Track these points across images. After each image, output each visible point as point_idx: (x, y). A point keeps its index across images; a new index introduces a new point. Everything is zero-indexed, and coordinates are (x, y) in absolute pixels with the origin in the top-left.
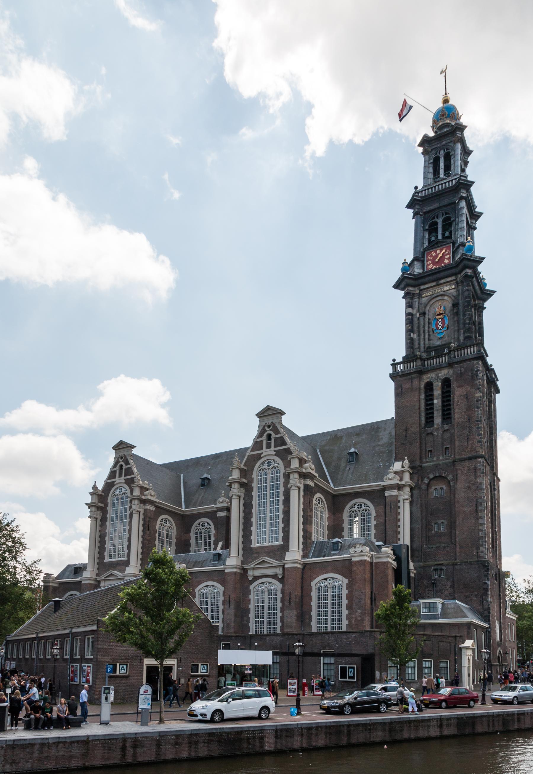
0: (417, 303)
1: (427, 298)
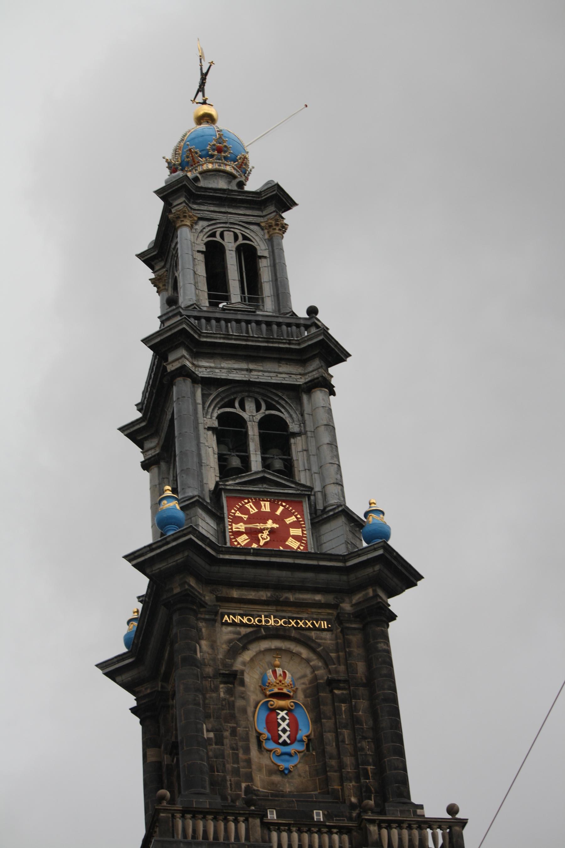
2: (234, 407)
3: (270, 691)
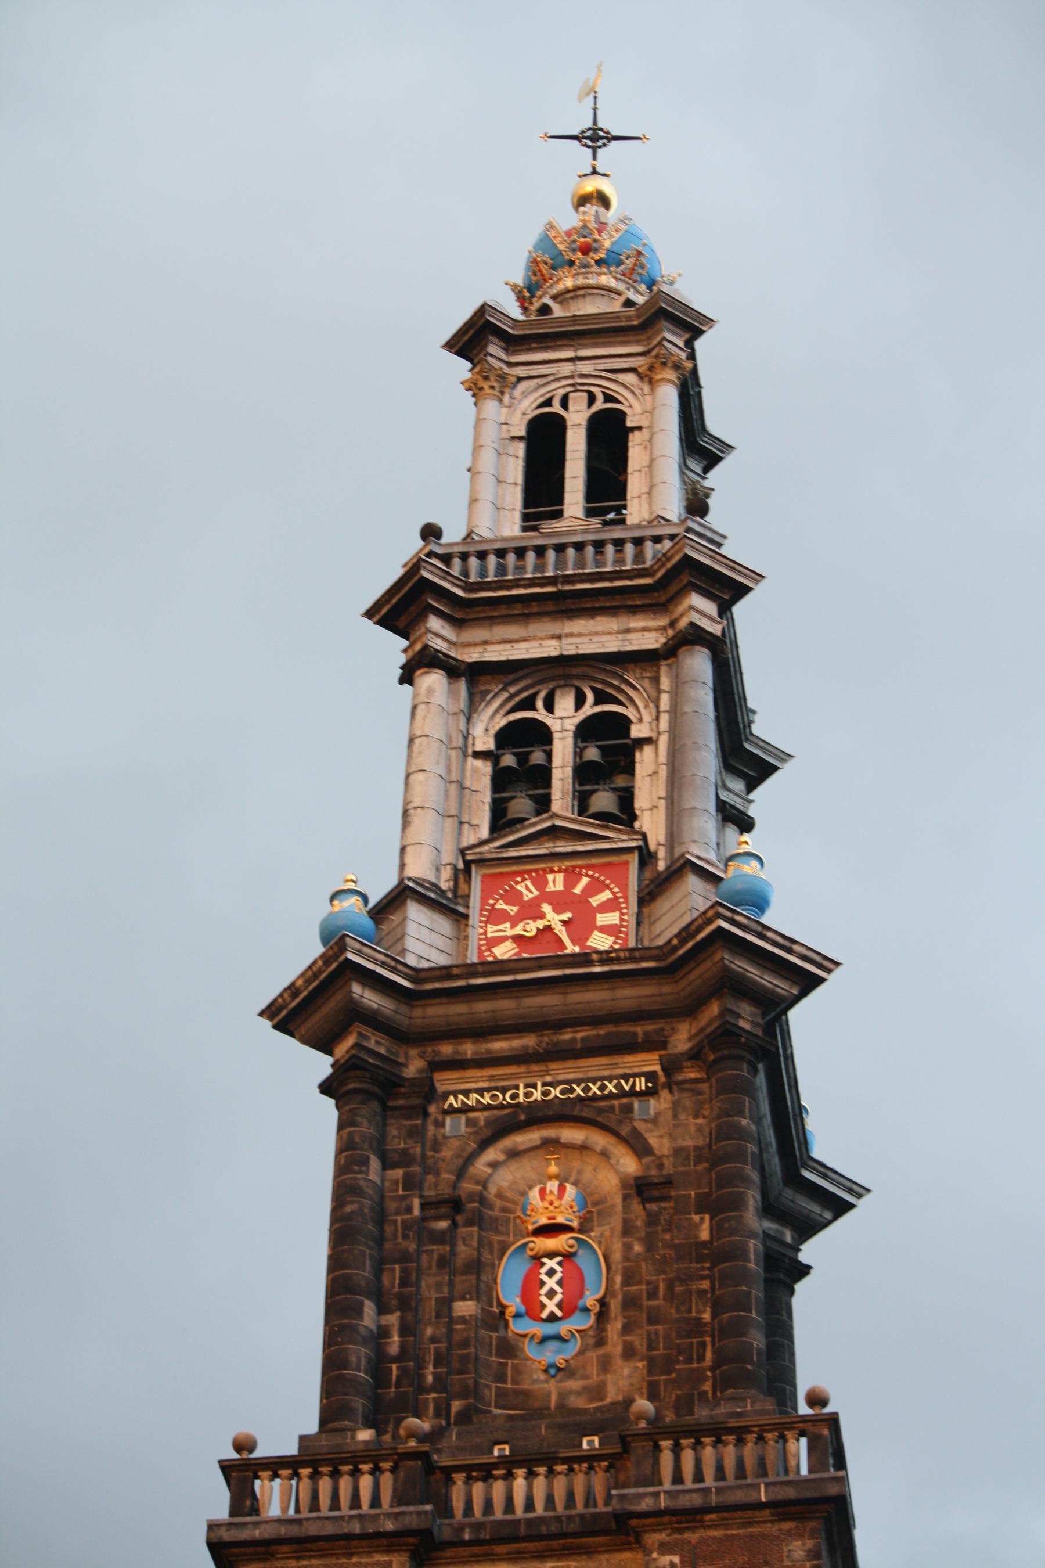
2: (534, 709)
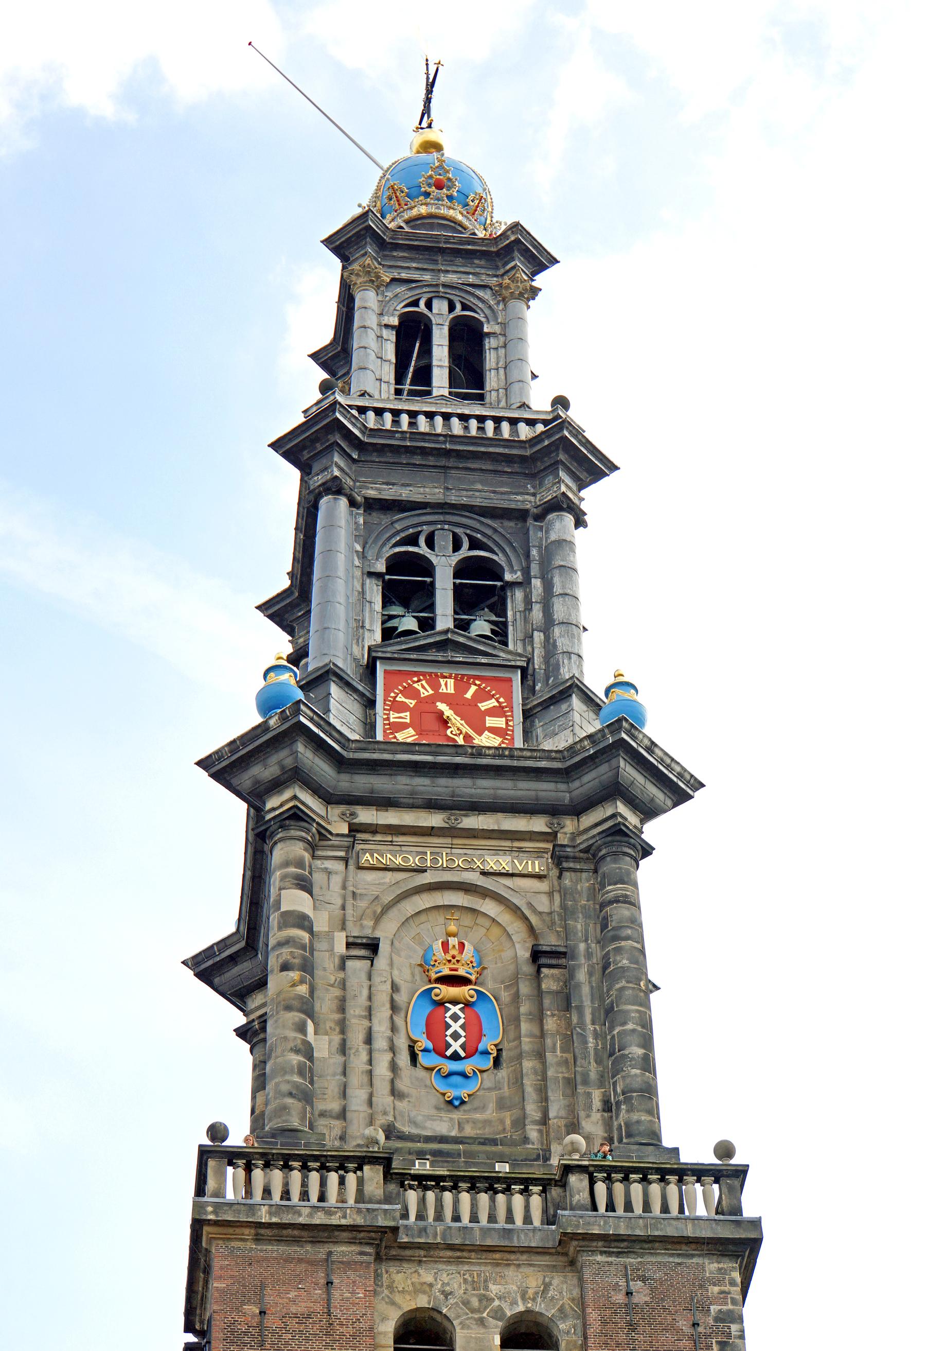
0: (336, 880)
1: (389, 877)
3: (437, 973)
